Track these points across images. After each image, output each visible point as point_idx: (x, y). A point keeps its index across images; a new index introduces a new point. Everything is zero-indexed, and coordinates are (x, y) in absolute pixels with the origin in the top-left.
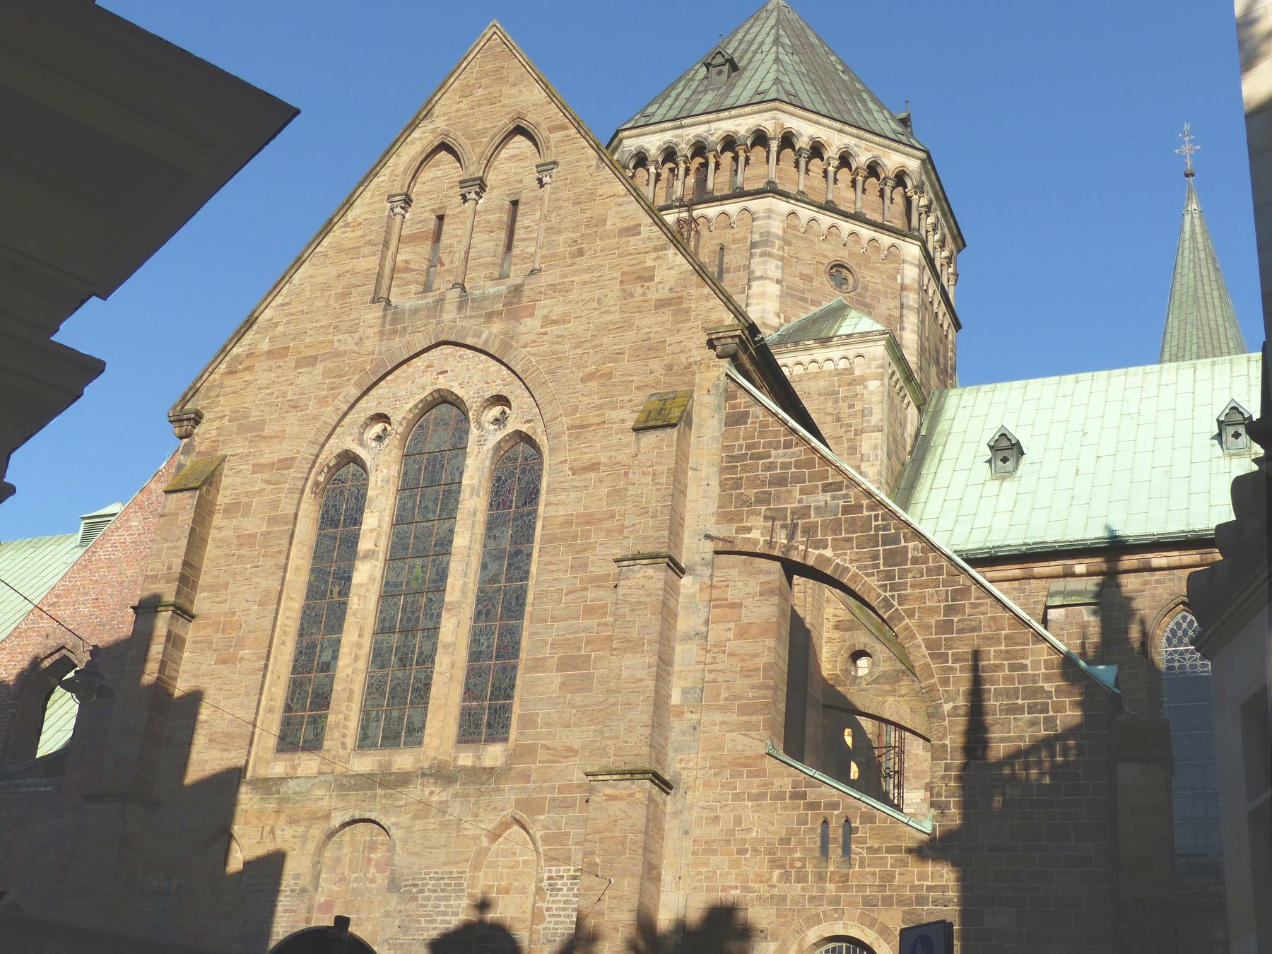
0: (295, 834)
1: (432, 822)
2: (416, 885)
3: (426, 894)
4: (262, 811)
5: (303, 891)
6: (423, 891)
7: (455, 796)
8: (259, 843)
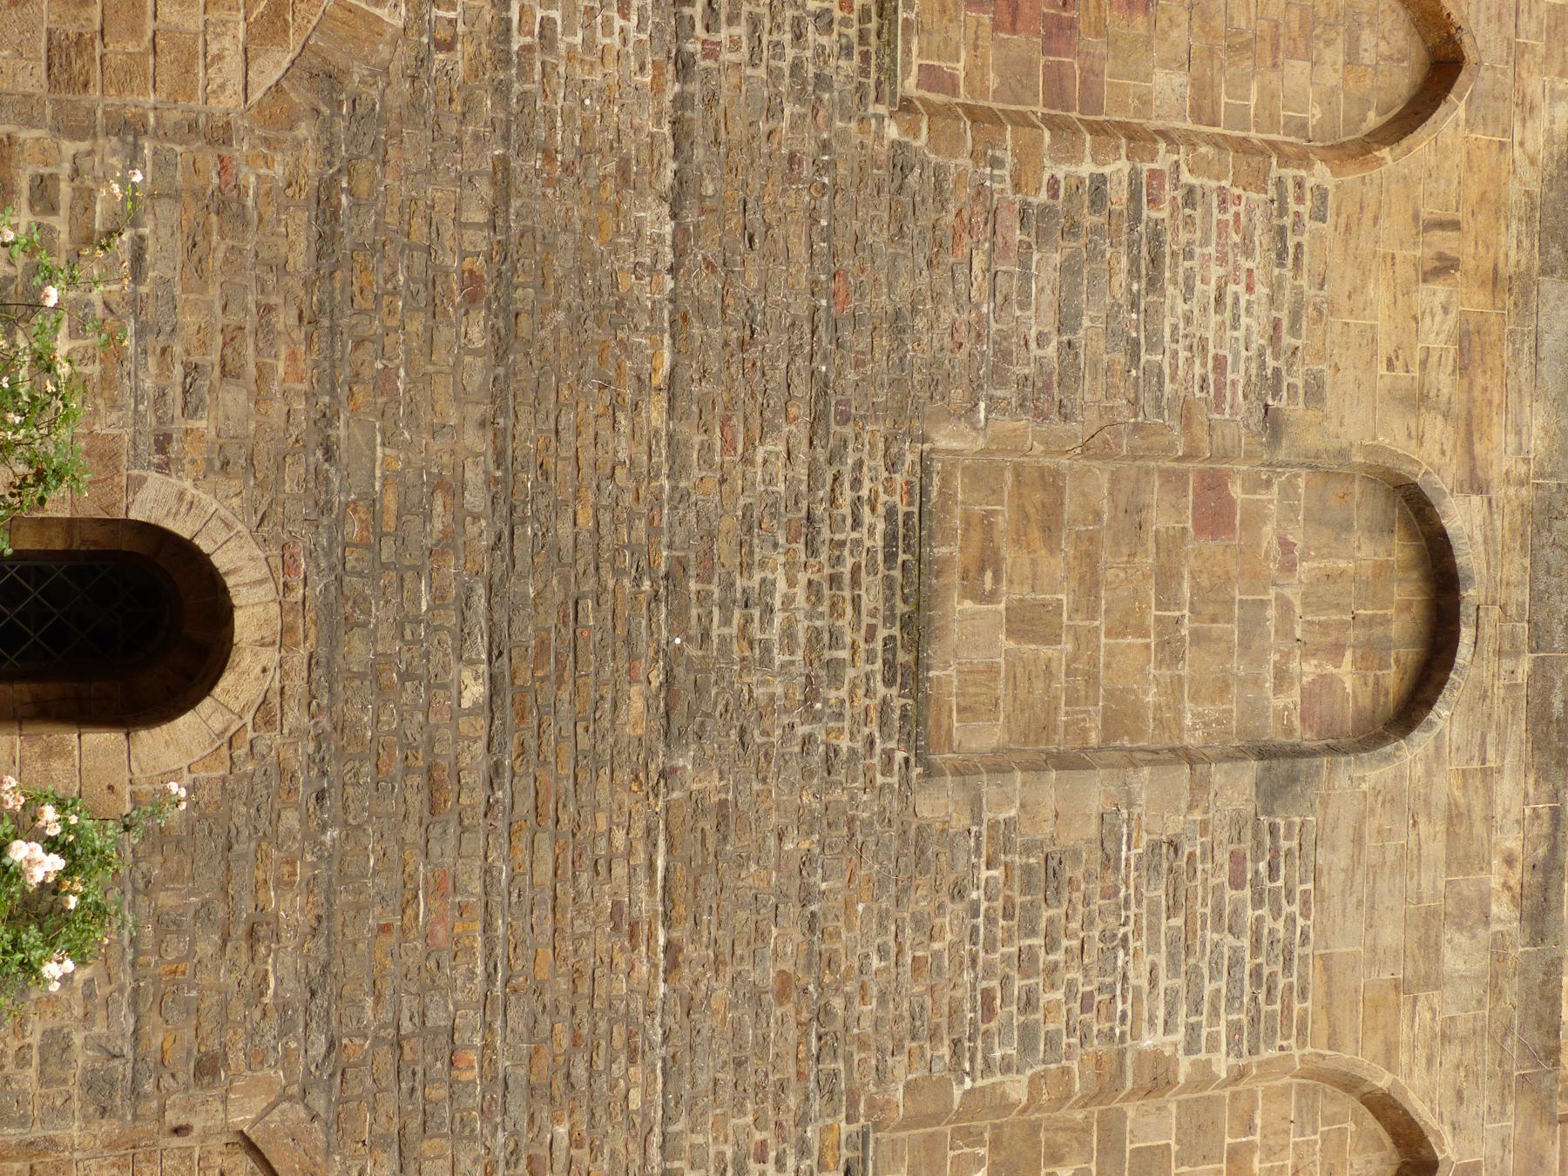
0: (1433, 360)
1: (1432, 881)
2: (1273, 870)
3: (1250, 914)
4: (1499, 211)
5: (1272, 423)
6: (1258, 903)
7: (1498, 947)
8: (1416, 217)
